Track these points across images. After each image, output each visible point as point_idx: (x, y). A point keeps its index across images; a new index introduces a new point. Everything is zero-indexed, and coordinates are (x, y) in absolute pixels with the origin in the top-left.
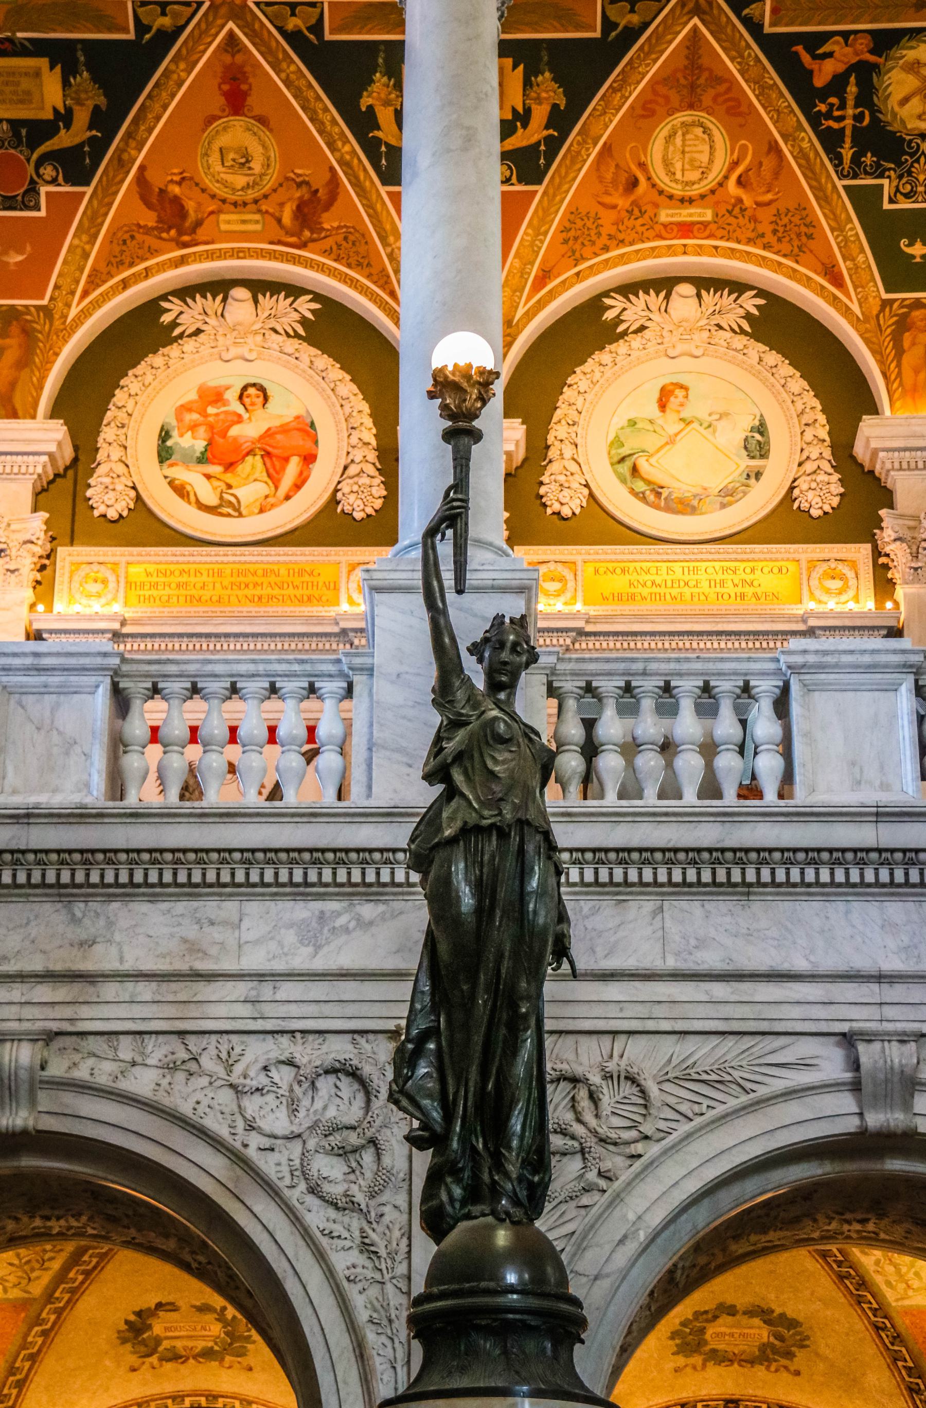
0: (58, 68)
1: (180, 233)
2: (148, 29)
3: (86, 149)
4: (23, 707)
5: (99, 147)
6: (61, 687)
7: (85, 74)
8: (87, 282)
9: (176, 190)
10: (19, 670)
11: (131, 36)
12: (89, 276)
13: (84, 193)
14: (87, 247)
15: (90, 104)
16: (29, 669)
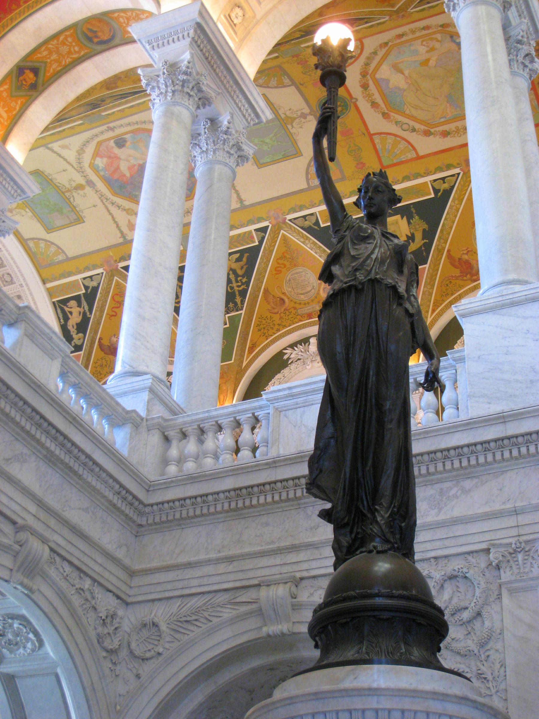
0: (405, 218)
1: (472, 276)
2: (439, 191)
3: (423, 248)
4: (287, 417)
5: (428, 246)
6: (305, 402)
7: (417, 217)
8: (433, 306)
9: (466, 257)
10: (282, 398)
11: (433, 196)
12: (434, 303)
13: (425, 267)
14: (430, 290)
15: (421, 229)
16: (287, 397)
